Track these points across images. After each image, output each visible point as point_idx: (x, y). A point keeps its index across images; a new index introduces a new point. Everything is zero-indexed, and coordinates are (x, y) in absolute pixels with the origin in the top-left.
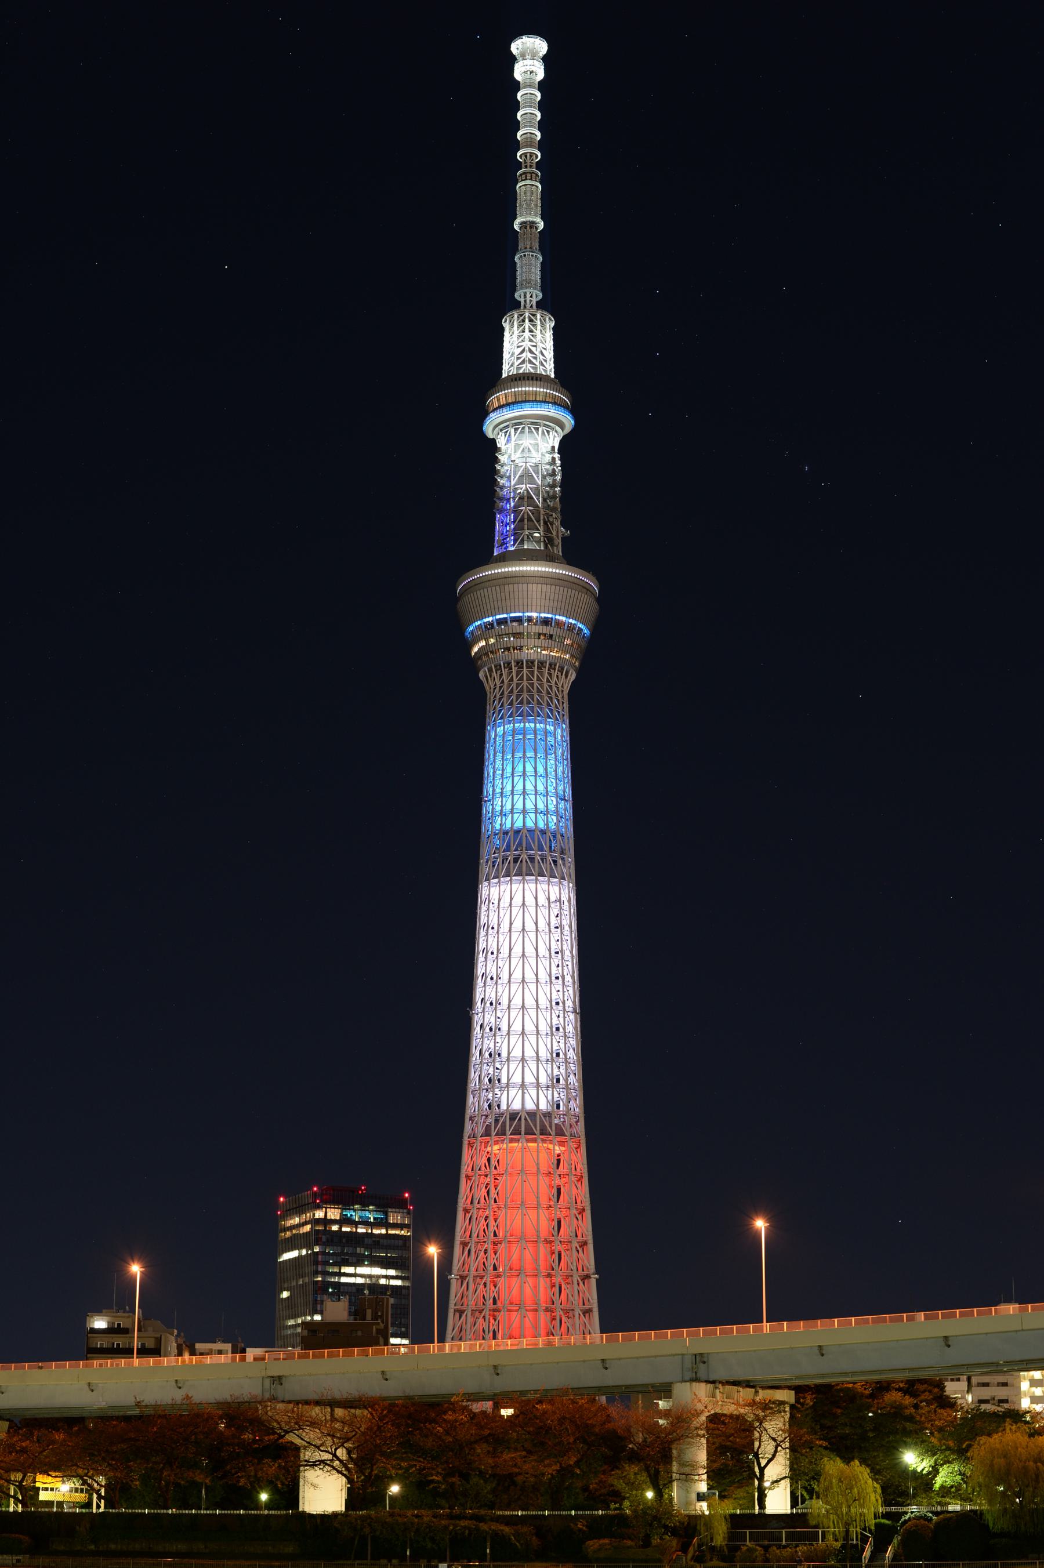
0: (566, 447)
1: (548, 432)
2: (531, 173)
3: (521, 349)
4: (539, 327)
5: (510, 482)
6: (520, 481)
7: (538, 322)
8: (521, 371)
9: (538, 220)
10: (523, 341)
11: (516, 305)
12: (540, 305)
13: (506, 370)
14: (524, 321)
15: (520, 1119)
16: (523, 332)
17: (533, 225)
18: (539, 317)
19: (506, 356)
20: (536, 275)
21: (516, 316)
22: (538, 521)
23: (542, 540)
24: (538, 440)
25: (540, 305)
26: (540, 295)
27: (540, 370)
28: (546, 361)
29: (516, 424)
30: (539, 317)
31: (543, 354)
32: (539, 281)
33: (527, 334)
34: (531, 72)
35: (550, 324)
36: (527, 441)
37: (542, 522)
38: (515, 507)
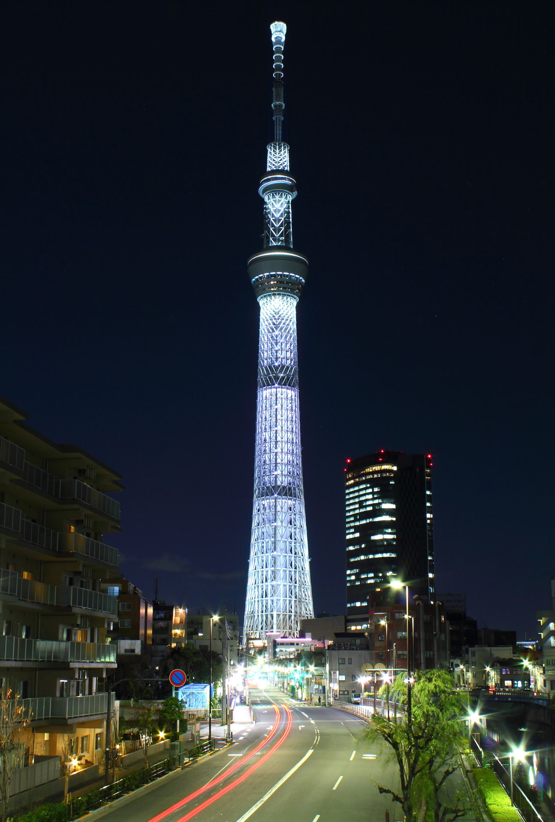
0: (294, 203)
3: (280, 159)
8: (280, 169)
13: (270, 167)
16: (281, 151)
17: (280, 106)
21: (277, 144)
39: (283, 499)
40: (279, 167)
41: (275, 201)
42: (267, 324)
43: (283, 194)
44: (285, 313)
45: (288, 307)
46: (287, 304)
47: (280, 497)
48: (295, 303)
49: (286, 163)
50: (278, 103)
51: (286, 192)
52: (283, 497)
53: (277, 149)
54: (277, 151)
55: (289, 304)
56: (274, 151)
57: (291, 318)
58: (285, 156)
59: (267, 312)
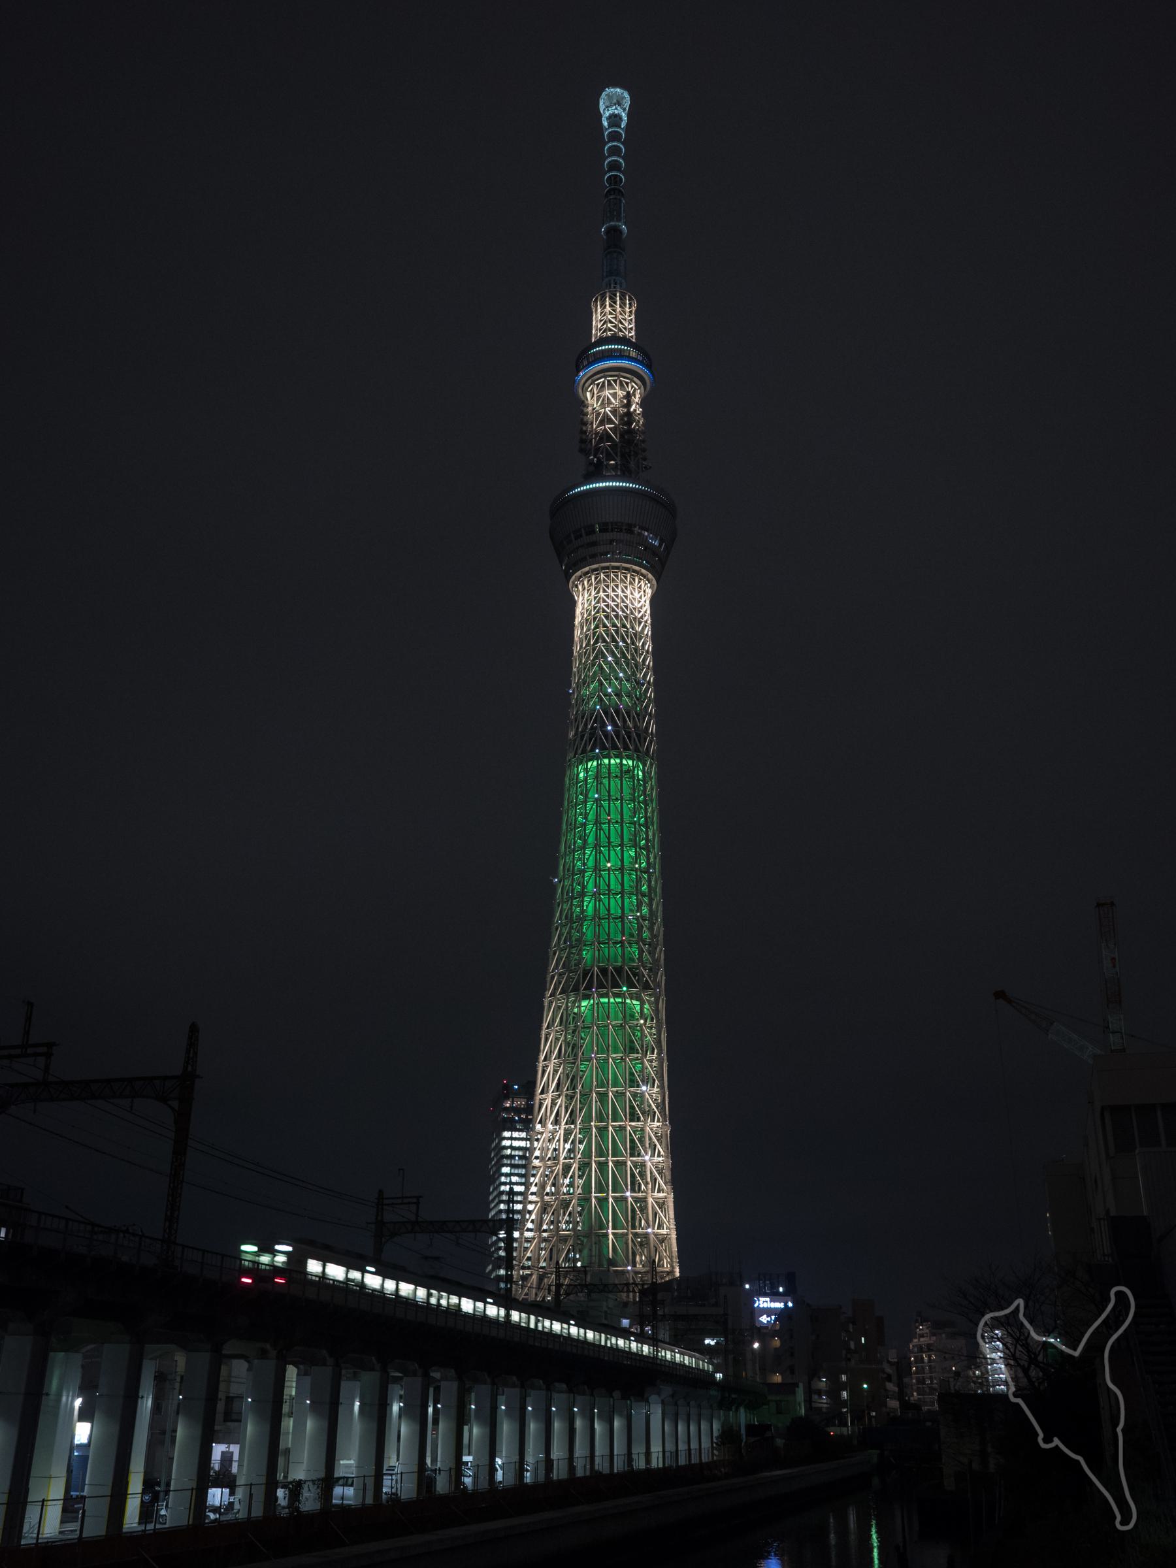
1: (627, 384)
4: (618, 303)
5: (593, 425)
6: (602, 423)
7: (618, 298)
10: (605, 315)
14: (606, 298)
15: (592, 974)
16: (605, 307)
18: (618, 294)
22: (617, 455)
23: (619, 467)
24: (616, 389)
28: (625, 329)
31: (622, 324)
33: (608, 309)
36: (607, 393)
37: (619, 454)
38: (595, 446)
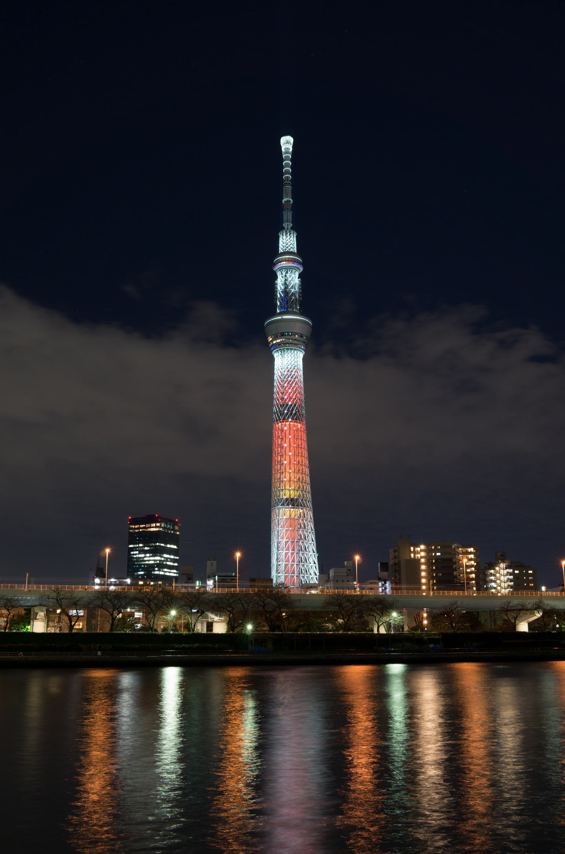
2: (287, 183)
9: (291, 200)
11: (283, 228)
12: (292, 228)
13: (281, 251)
17: (289, 201)
19: (280, 245)
20: (290, 218)
25: (292, 228)
26: (292, 225)
27: (292, 250)
29: (287, 268)
30: (292, 232)
32: (291, 220)
34: (287, 148)
35: (295, 236)
39: (286, 508)
40: (286, 250)
41: (282, 277)
42: (277, 373)
43: (288, 270)
44: (289, 363)
45: (292, 358)
46: (291, 356)
47: (283, 507)
48: (300, 355)
49: (291, 246)
50: (287, 199)
51: (291, 268)
52: (287, 507)
53: (284, 236)
54: (284, 237)
55: (292, 356)
56: (282, 238)
57: (295, 366)
58: (291, 240)
59: (277, 364)
